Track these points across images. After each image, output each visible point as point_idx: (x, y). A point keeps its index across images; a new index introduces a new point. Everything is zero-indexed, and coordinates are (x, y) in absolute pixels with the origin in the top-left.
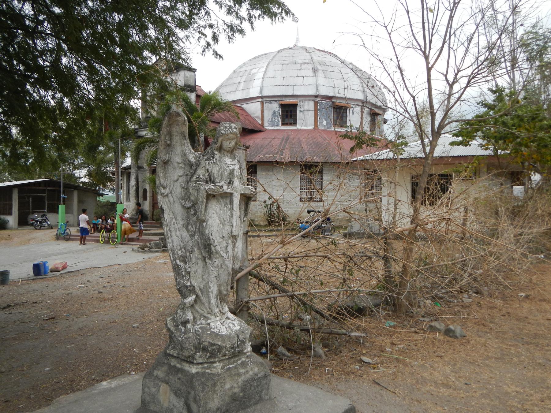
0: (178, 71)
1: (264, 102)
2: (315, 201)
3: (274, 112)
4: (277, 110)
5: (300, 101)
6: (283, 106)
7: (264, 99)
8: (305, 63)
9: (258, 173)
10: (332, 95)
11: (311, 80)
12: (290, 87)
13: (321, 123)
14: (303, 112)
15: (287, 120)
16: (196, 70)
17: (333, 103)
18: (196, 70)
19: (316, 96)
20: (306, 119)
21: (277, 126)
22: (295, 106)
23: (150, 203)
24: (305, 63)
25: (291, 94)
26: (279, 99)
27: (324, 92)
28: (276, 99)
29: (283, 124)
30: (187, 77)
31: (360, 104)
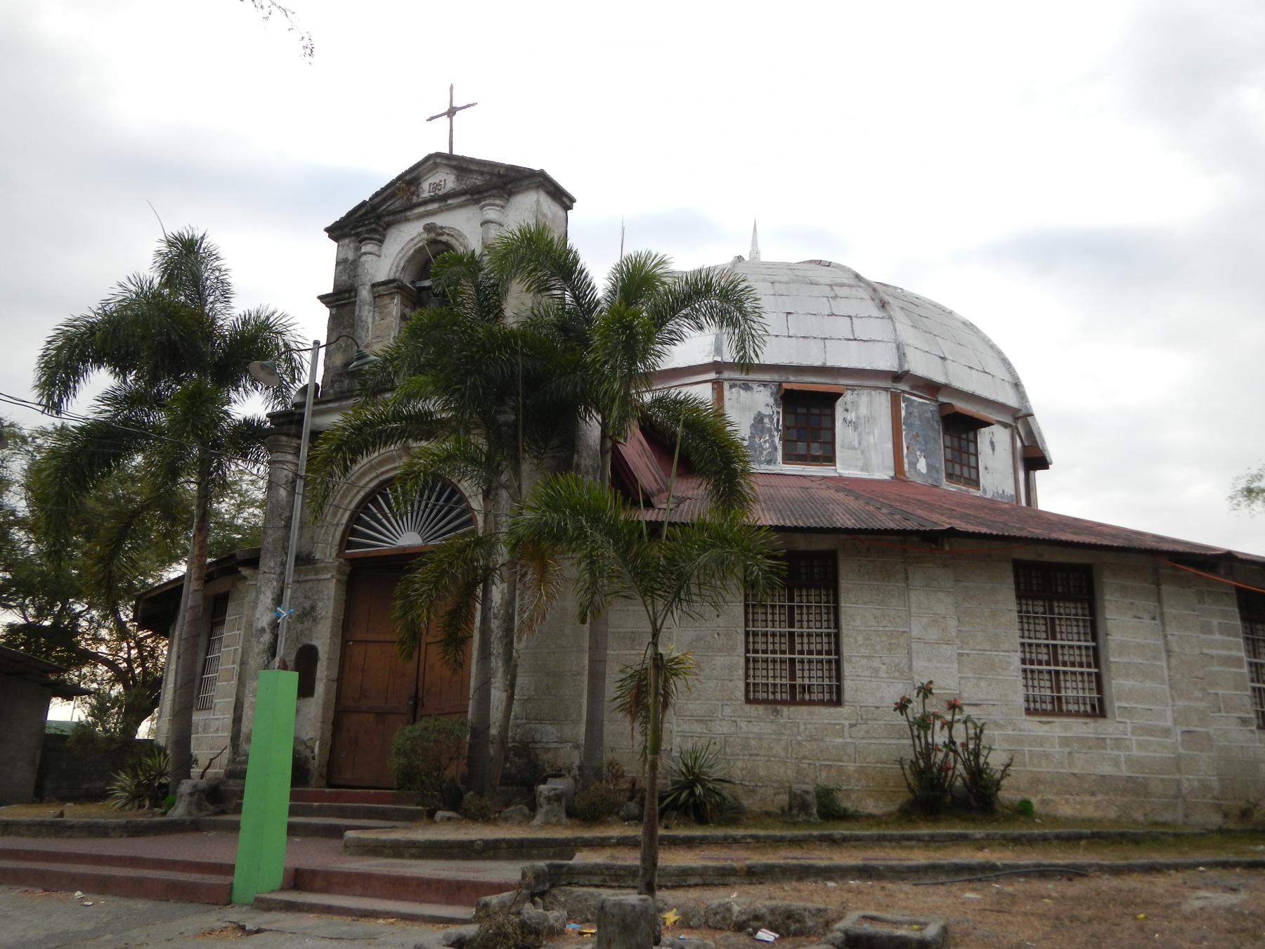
0: (511, 194)
1: (726, 385)
2: (1077, 714)
3: (759, 419)
4: (767, 411)
5: (848, 387)
6: (791, 400)
7: (726, 375)
8: (842, 285)
9: (847, 583)
10: (939, 378)
11: (874, 327)
12: (812, 341)
13: (913, 464)
14: (855, 425)
15: (801, 448)
16: (573, 200)
17: (942, 405)
18: (573, 200)
19: (897, 377)
20: (866, 445)
21: (769, 462)
22: (829, 400)
23: (325, 709)
24: (842, 285)
25: (818, 363)
26: (776, 377)
27: (921, 366)
28: (767, 377)
29: (788, 458)
30: (545, 216)
31: (1009, 420)
